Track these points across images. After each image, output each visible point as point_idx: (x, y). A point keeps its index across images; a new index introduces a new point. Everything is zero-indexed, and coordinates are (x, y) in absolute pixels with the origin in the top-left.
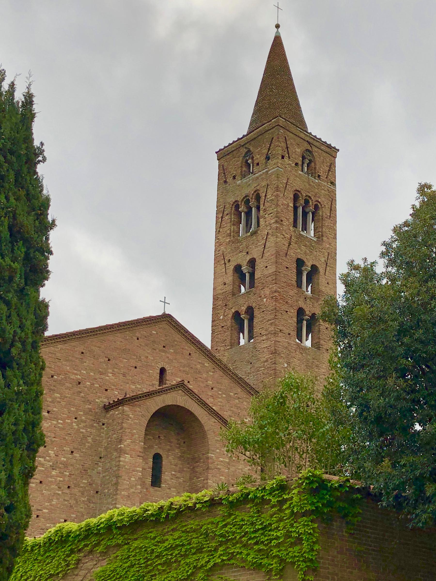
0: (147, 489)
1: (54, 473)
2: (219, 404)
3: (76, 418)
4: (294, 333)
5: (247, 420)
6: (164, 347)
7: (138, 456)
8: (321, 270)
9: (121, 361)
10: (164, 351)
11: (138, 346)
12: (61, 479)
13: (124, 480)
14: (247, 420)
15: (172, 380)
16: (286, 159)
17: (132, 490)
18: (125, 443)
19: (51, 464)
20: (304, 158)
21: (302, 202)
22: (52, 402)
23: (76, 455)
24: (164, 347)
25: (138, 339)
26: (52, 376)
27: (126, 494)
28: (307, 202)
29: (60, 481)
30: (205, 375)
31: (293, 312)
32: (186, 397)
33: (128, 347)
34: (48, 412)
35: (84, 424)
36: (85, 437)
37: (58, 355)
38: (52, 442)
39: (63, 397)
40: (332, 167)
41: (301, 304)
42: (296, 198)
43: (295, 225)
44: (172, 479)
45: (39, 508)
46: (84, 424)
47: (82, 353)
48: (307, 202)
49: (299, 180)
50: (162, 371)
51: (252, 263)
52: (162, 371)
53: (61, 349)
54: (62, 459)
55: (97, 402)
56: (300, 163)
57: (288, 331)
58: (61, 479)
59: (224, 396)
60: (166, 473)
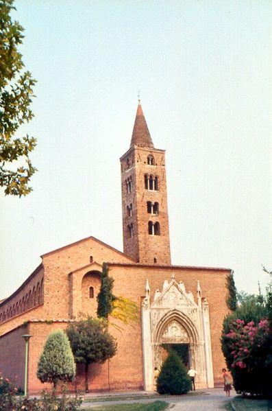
4: (147, 232)
8: (160, 203)
15: (94, 260)
16: (139, 162)
20: (148, 159)
21: (149, 177)
23: (60, 292)
28: (151, 177)
31: (147, 223)
36: (62, 286)
39: (53, 273)
40: (163, 159)
41: (150, 220)
42: (146, 176)
43: (146, 188)
48: (151, 177)
49: (149, 169)
50: (91, 257)
51: (131, 205)
52: (91, 257)
56: (147, 162)
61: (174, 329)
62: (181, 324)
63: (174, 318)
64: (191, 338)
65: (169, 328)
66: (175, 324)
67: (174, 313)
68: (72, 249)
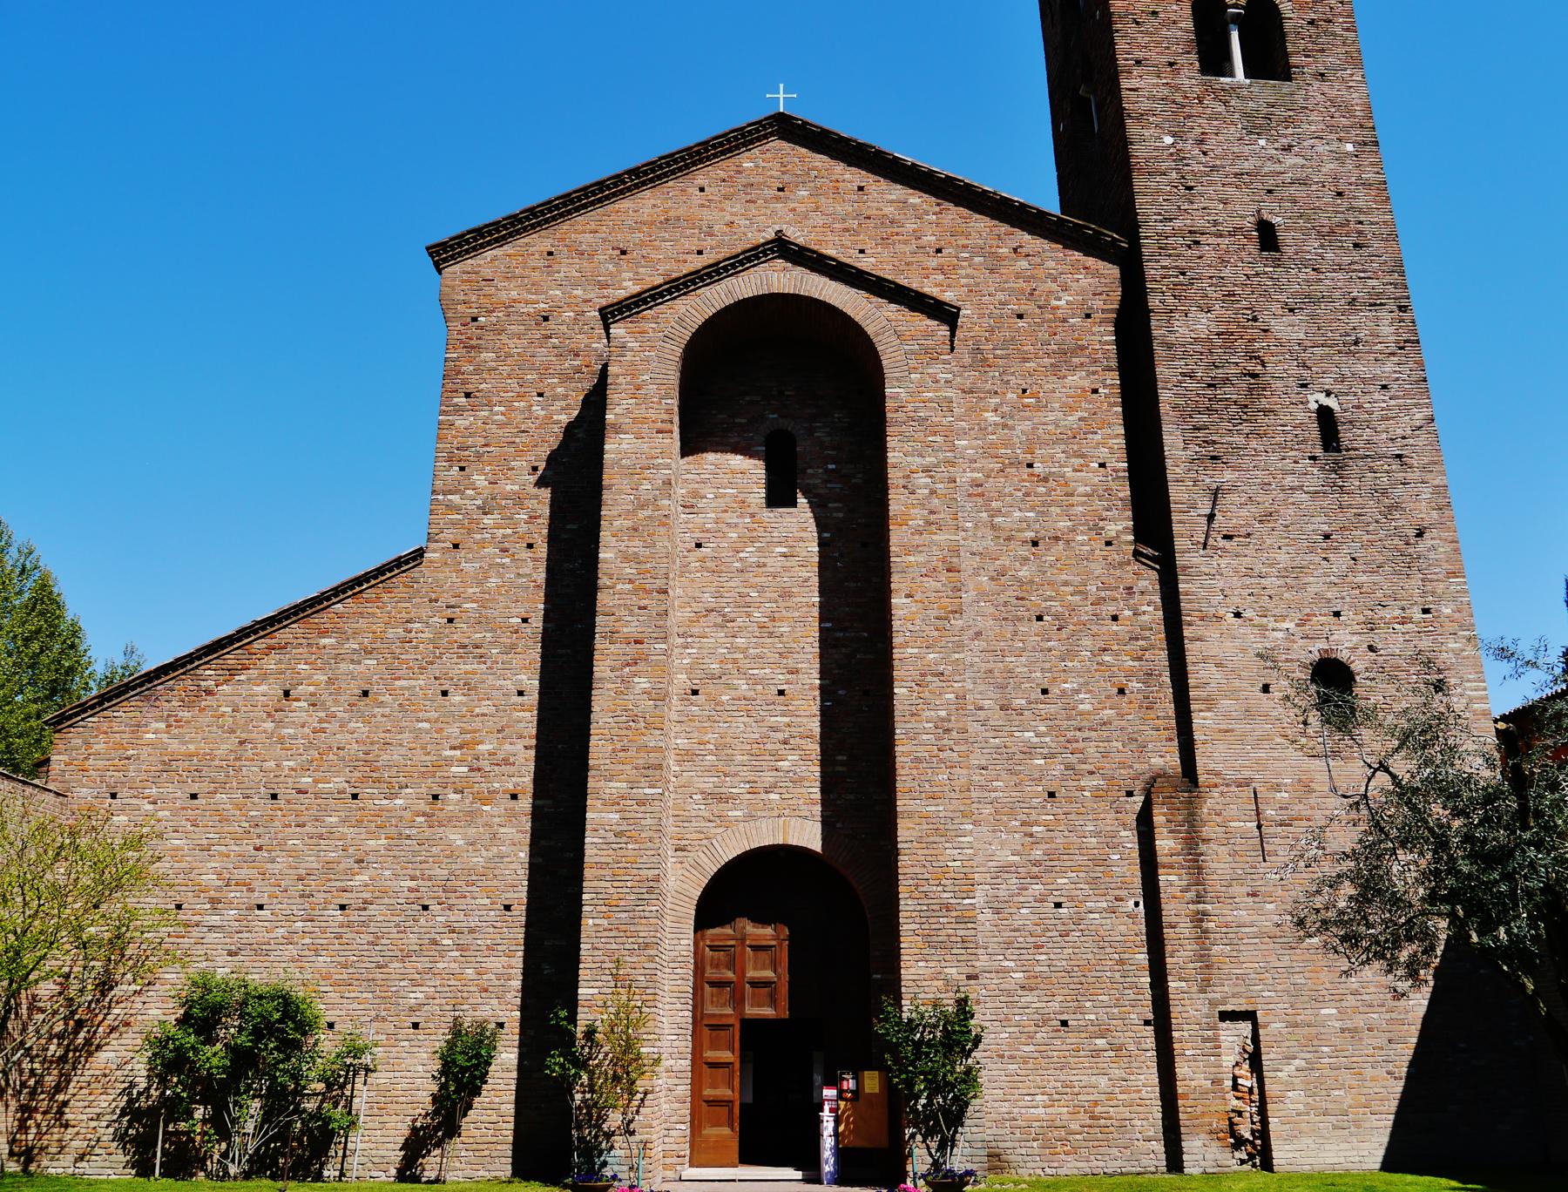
0: (752, 516)
1: (487, 521)
2: (963, 281)
3: (540, 395)
5: (1063, 302)
6: (781, 190)
7: (659, 432)
9: (657, 249)
10: (778, 199)
11: (703, 206)
12: (509, 531)
13: (620, 492)
14: (1063, 302)
17: (642, 514)
18: (618, 410)
19: (479, 502)
22: (477, 371)
24: (781, 190)
25: (702, 190)
26: (475, 319)
27: (628, 523)
29: (504, 536)
30: (910, 227)
32: (799, 271)
33: (672, 214)
34: (468, 395)
35: (563, 403)
37: (487, 272)
38: (479, 456)
44: (829, 481)
45: (453, 601)
46: (563, 403)
47: (550, 254)
53: (495, 259)
54: (508, 488)
55: (596, 350)
57: (1165, 59)
58: (509, 531)
59: (977, 260)
60: (810, 471)
68: (646, 203)
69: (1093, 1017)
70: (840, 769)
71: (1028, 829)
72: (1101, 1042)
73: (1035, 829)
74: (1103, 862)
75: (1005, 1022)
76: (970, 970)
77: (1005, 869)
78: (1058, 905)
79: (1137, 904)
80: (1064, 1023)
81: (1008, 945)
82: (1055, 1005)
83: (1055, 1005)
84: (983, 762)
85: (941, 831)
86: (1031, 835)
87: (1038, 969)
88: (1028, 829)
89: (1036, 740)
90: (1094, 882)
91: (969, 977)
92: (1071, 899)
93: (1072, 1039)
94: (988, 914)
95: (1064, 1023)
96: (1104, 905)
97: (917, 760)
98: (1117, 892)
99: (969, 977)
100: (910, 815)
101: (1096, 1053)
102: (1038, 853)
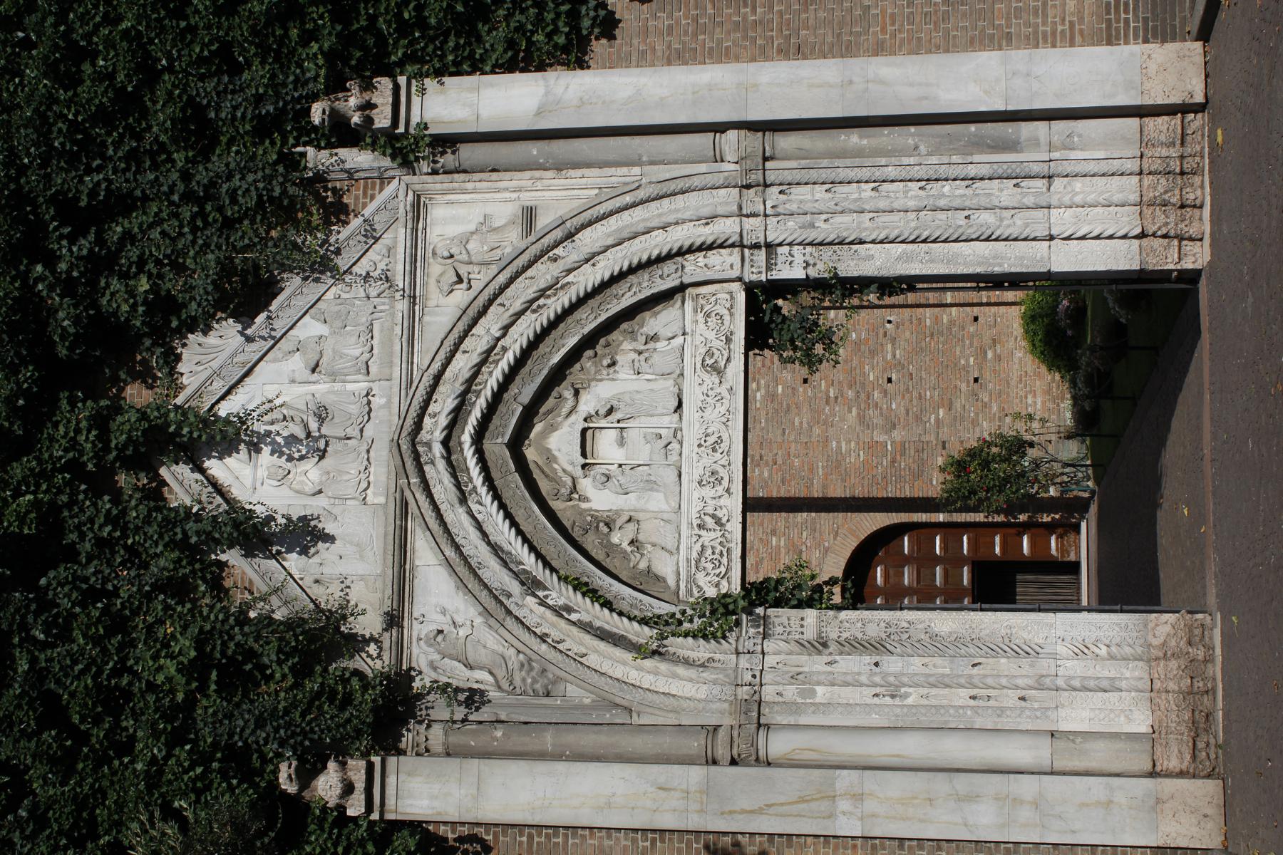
61: (607, 447)
62: (557, 375)
63: (497, 446)
64: (694, 267)
65: (600, 499)
66: (557, 443)
67: (453, 469)
69: (972, 359)
70: (782, 543)
71: (832, 400)
72: (990, 354)
73: (832, 395)
74: (858, 344)
75: (975, 423)
76: (940, 447)
77: (861, 418)
78: (890, 380)
79: (889, 322)
80: (976, 380)
81: (918, 419)
82: (963, 386)
83: (963, 386)
84: (780, 432)
85: (837, 463)
86: (836, 398)
87: (936, 398)
88: (832, 400)
89: (763, 391)
90: (873, 353)
91: (944, 448)
92: (884, 370)
93: (987, 375)
94: (895, 434)
95: (976, 380)
96: (889, 346)
97: (783, 482)
98: (881, 335)
99: (944, 448)
100: (825, 487)
101: (998, 358)
102: (850, 394)
